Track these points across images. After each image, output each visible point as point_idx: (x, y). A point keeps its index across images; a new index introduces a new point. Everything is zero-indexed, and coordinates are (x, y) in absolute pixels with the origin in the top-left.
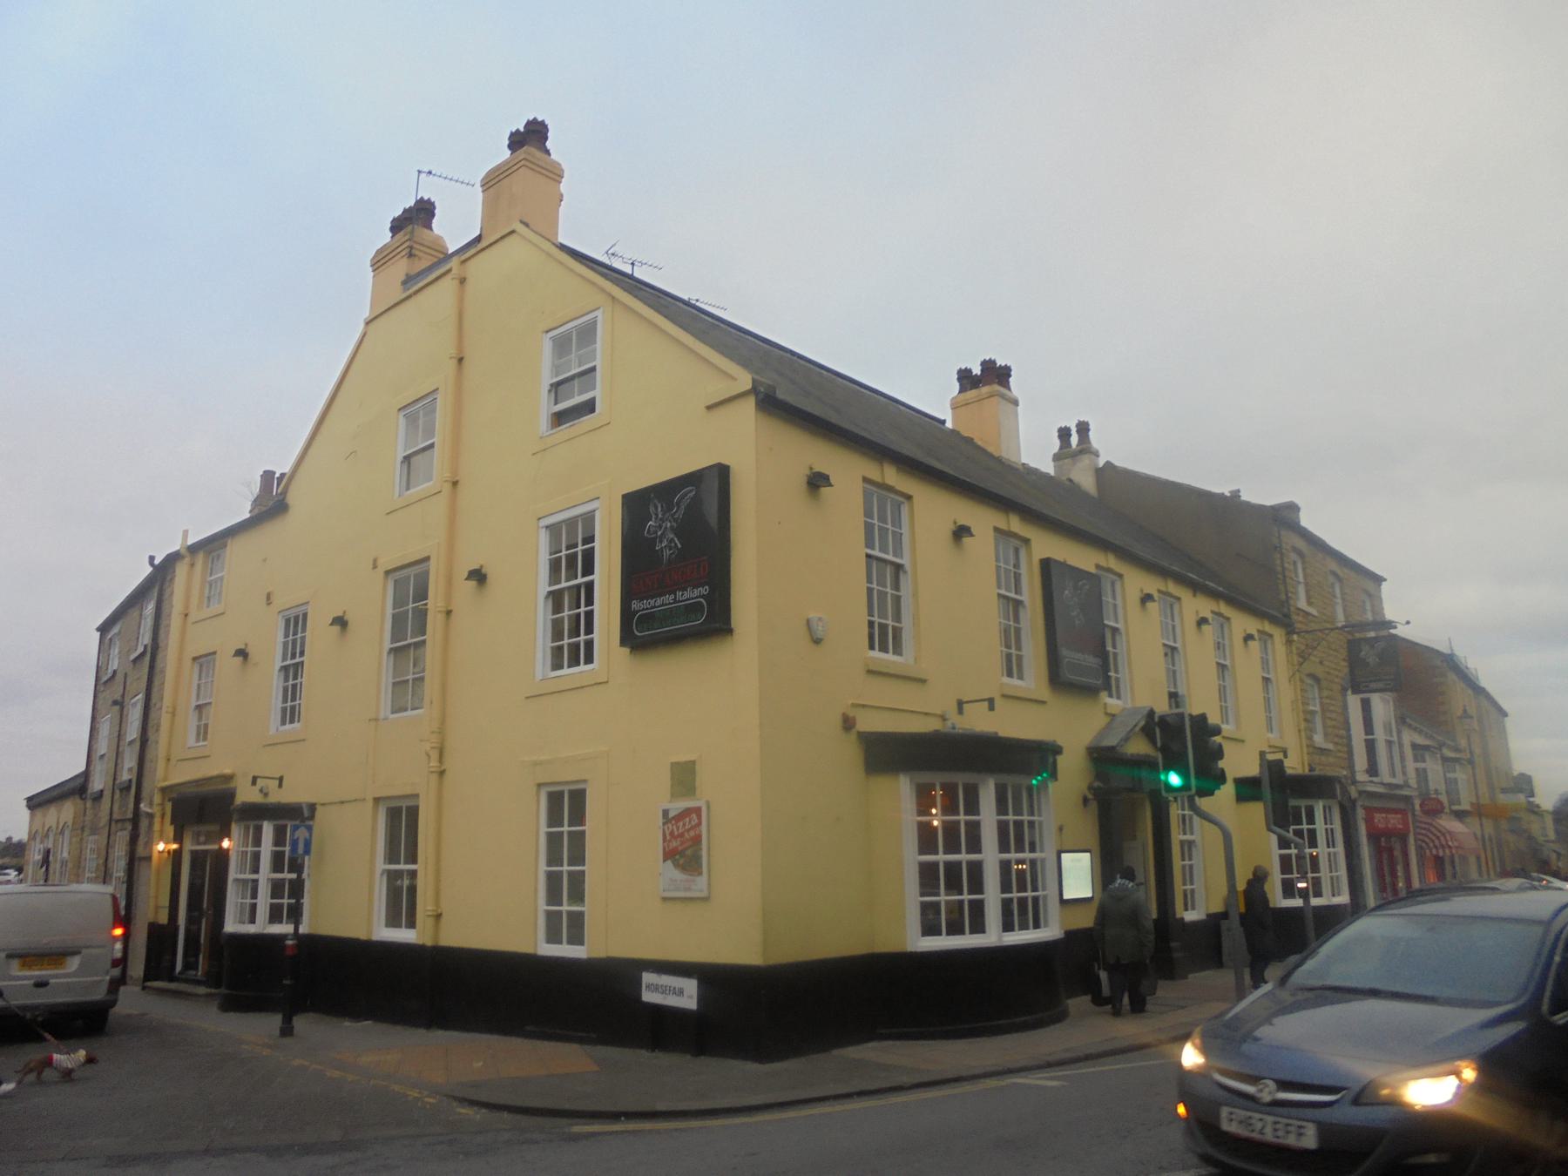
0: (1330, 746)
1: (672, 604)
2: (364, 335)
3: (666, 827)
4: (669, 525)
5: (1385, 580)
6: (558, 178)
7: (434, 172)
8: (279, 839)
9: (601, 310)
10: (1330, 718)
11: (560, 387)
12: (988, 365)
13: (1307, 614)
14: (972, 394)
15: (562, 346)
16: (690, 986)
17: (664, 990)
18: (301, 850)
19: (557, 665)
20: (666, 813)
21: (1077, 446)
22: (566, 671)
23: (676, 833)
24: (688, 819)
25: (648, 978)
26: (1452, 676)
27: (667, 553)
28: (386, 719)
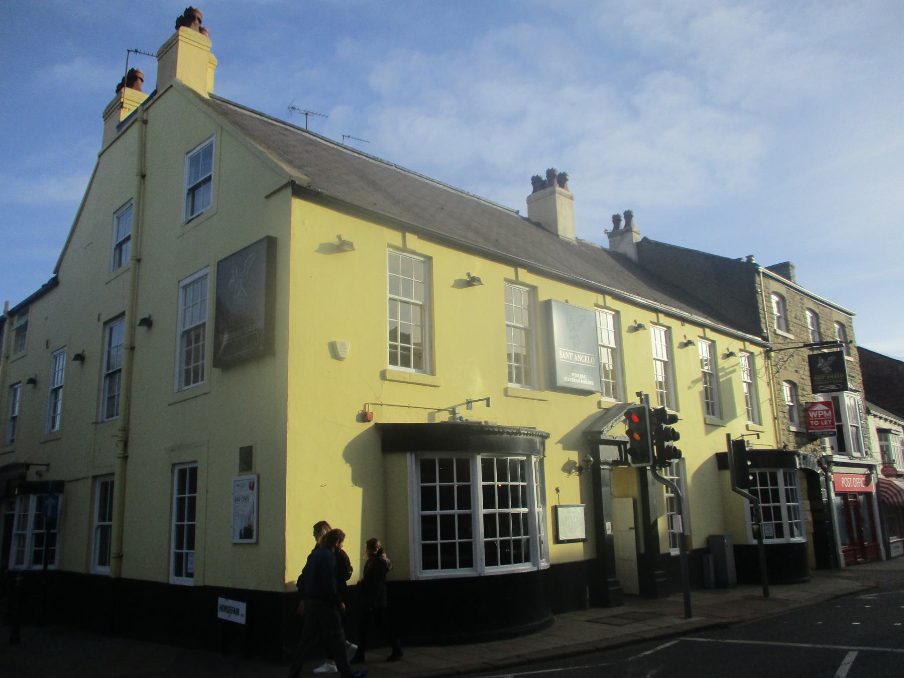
2: (98, 164)
7: (139, 51)
8: (40, 505)
9: (215, 135)
11: (197, 192)
12: (551, 173)
15: (195, 161)
16: (242, 607)
22: (192, 385)
28: (102, 422)
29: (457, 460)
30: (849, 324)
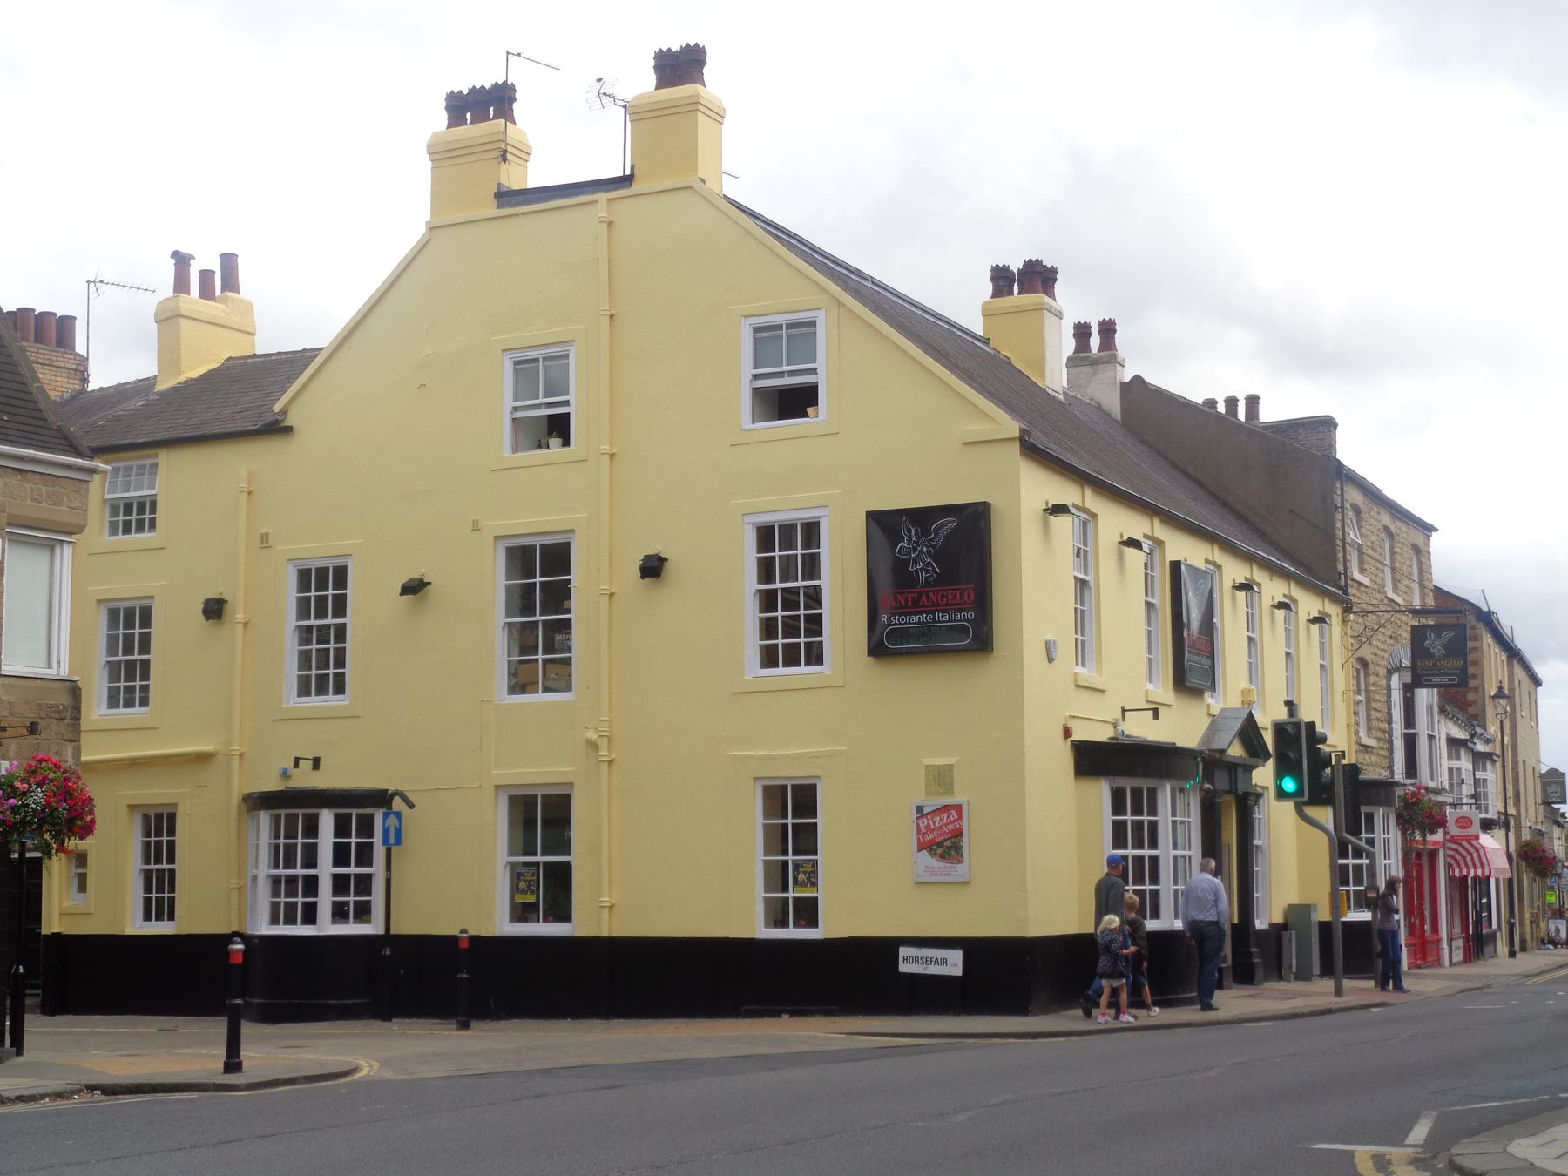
0: (1372, 742)
1: (930, 623)
3: (920, 822)
4: (925, 549)
5: (1436, 530)
6: (719, 119)
8: (341, 828)
10: (1375, 709)
13: (1361, 584)
14: (1005, 302)
17: (925, 961)
18: (392, 840)
19: (769, 658)
20: (920, 809)
21: (1099, 351)
23: (932, 827)
24: (946, 815)
25: (904, 951)
26: (1487, 640)
27: (922, 576)
29: (1147, 789)
30: (1426, 548)
